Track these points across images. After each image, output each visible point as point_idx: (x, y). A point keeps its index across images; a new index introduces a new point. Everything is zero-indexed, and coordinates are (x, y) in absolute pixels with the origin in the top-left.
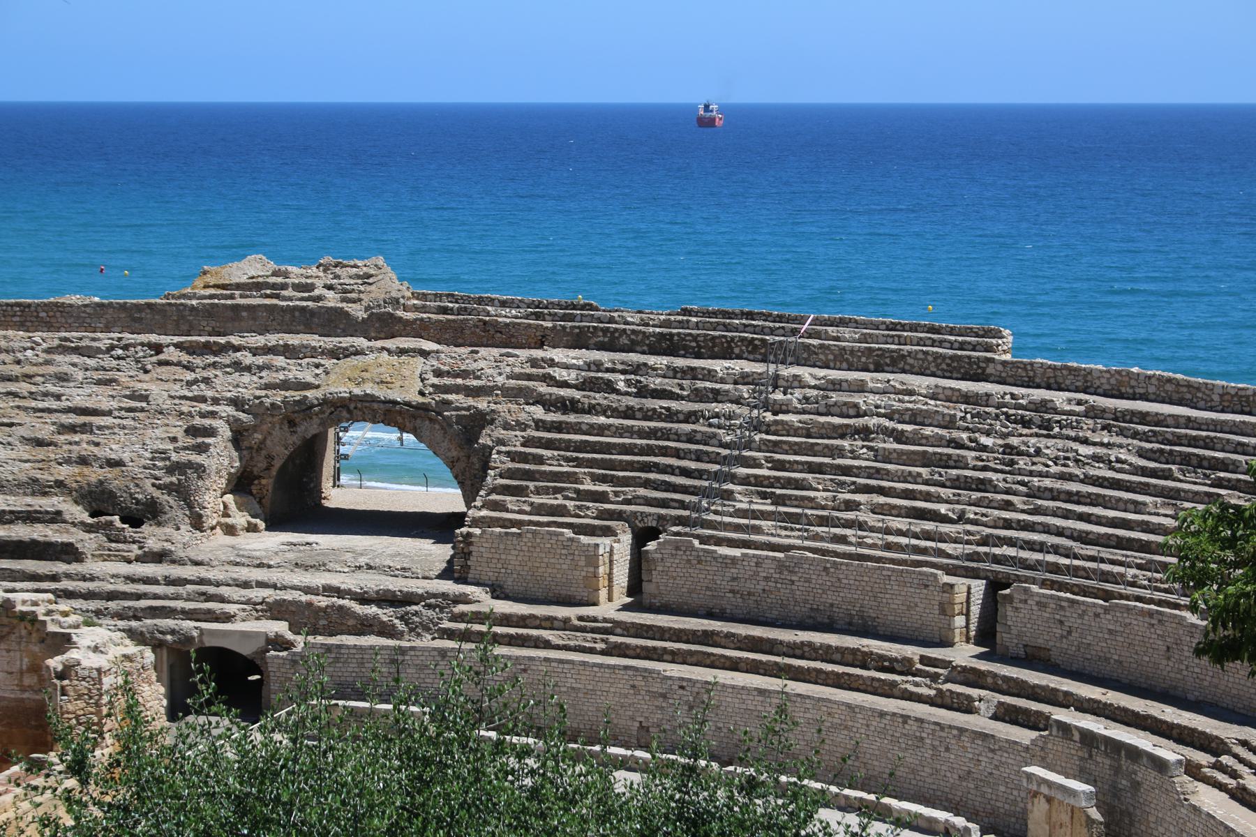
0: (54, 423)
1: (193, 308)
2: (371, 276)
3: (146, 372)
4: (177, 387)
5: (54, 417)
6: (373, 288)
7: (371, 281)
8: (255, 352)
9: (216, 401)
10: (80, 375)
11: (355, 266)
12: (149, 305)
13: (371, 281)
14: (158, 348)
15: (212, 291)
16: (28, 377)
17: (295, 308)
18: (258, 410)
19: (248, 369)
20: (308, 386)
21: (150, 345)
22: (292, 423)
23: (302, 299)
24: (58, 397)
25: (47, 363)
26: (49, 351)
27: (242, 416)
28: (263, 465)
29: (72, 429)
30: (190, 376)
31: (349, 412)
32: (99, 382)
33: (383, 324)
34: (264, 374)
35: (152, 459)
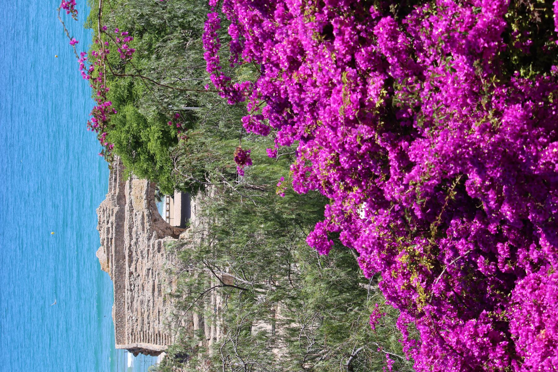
0: (158, 298)
1: (116, 267)
2: (104, 210)
3: (139, 275)
4: (144, 262)
5: (156, 299)
6: (108, 207)
7: (105, 209)
8: (131, 239)
9: (149, 246)
10: (141, 297)
11: (100, 217)
12: (116, 282)
13: (105, 209)
14: (131, 273)
15: (110, 264)
16: (142, 314)
17: (116, 231)
18: (151, 230)
19: (137, 239)
20: (143, 216)
21: (130, 276)
22: (155, 220)
23: (112, 230)
24: (149, 301)
25: (137, 310)
26: (132, 312)
27: (154, 235)
28: (169, 230)
29: (160, 291)
30: (140, 259)
31: (151, 200)
32: (143, 290)
33: (121, 199)
34: (139, 233)
35: (169, 260)
